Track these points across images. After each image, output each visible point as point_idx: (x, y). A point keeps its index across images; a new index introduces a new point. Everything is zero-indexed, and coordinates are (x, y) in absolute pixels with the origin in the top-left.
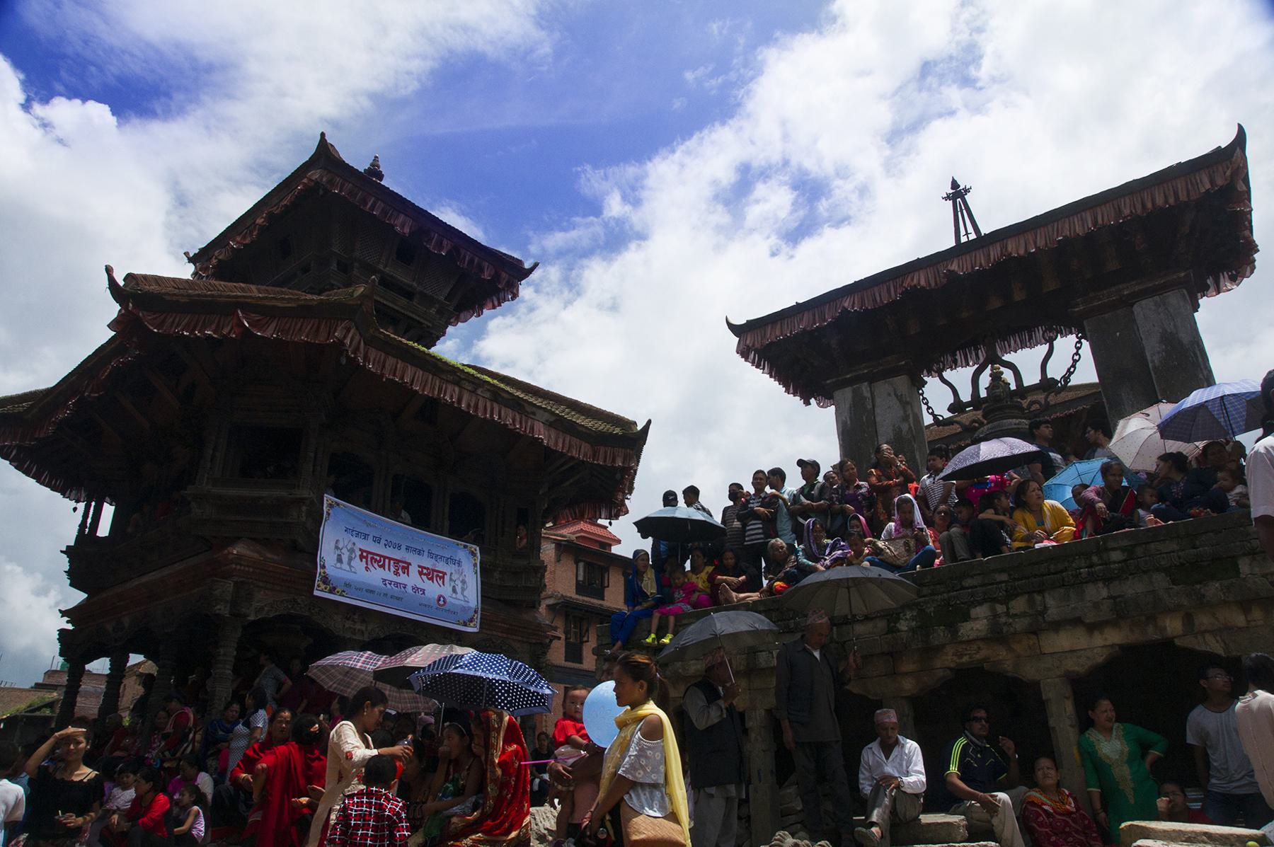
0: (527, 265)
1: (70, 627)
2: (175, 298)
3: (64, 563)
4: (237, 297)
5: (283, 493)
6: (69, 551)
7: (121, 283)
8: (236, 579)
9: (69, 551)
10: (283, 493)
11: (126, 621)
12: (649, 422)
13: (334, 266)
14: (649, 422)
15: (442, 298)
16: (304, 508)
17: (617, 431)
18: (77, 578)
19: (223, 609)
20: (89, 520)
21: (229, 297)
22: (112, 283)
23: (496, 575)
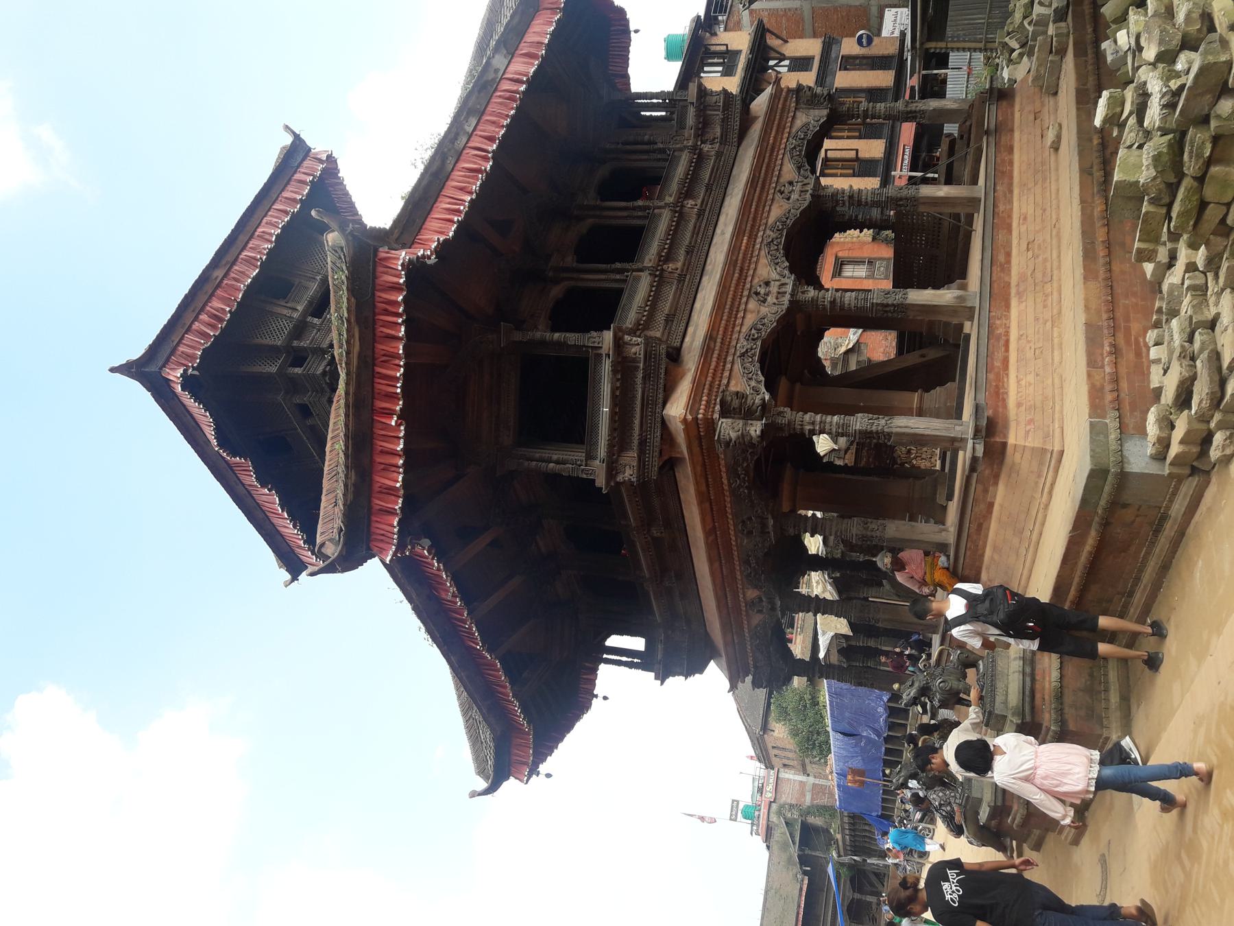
1: (749, 679)
2: (351, 489)
3: (675, 681)
4: (347, 406)
5: (606, 366)
6: (662, 677)
8: (716, 416)
9: (662, 677)
10: (606, 366)
11: (752, 594)
13: (298, 370)
16: (627, 338)
18: (694, 667)
19: (756, 429)
20: (624, 659)
21: (347, 415)
23: (706, 148)
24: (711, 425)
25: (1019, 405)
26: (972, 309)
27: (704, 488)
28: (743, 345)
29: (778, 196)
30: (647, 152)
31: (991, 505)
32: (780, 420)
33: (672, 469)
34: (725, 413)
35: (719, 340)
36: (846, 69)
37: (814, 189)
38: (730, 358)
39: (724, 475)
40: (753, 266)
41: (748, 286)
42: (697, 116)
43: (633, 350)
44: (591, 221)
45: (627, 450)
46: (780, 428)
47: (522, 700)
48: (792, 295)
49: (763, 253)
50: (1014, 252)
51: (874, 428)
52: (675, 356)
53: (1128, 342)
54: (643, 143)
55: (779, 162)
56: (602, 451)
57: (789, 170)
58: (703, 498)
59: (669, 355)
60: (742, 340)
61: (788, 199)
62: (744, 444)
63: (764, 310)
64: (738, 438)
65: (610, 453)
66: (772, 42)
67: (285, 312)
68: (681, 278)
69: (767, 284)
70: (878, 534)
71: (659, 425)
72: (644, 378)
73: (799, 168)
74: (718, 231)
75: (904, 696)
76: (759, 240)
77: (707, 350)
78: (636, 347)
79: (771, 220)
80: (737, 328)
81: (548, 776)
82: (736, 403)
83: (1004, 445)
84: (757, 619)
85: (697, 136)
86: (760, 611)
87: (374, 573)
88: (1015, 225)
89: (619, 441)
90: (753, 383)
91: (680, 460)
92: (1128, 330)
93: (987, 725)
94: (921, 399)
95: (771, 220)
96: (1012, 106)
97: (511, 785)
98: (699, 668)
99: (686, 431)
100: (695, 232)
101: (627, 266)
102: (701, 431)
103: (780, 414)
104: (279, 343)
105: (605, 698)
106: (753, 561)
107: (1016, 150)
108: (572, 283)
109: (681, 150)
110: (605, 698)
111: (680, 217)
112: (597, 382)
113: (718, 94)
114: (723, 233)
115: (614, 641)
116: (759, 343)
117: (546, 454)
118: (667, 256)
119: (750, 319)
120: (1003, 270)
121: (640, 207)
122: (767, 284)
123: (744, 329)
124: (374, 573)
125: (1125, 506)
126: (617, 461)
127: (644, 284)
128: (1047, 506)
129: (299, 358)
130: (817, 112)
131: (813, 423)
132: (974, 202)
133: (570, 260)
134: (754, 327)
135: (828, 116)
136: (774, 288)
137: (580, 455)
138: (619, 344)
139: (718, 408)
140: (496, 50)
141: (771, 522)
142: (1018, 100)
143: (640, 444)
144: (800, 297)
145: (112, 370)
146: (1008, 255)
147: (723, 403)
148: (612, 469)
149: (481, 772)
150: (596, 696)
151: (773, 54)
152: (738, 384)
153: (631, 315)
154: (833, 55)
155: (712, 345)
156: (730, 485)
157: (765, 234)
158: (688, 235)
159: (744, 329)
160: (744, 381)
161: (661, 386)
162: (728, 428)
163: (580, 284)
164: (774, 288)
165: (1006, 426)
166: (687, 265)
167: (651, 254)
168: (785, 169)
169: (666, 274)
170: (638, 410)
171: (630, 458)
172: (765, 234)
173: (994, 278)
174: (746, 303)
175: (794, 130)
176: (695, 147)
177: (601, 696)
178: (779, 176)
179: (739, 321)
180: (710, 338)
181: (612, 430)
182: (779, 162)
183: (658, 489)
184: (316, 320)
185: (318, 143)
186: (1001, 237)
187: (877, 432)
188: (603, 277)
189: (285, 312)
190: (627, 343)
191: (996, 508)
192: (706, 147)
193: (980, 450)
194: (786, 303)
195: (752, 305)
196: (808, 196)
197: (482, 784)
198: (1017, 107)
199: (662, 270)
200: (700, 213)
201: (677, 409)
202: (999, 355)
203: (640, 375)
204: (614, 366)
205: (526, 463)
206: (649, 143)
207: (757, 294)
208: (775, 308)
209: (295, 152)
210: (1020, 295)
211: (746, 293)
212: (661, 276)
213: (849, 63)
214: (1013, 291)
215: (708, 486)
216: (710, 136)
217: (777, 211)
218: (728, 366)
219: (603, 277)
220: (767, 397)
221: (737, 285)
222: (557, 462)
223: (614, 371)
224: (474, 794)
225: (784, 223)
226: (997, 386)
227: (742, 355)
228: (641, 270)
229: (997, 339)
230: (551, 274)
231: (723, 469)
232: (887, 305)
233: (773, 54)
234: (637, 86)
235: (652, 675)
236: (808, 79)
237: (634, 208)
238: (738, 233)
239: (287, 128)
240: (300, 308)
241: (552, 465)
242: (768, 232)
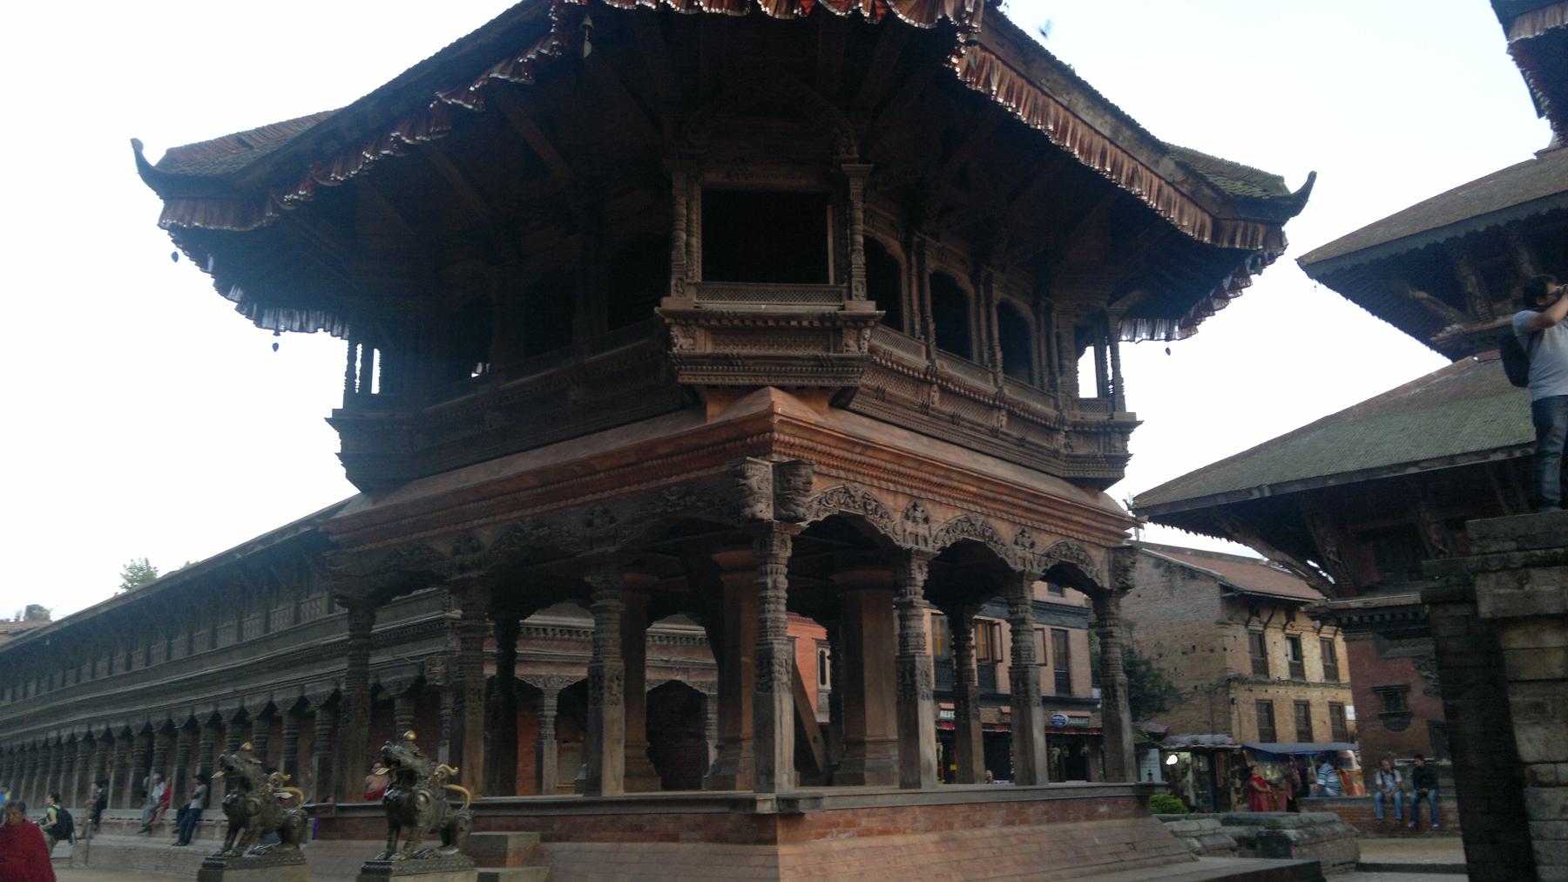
3: (332, 441)
5: (829, 308)
6: (337, 420)
8: (776, 458)
9: (337, 420)
11: (486, 537)
12: (1312, 177)
14: (1312, 177)
17: (1257, 192)
19: (764, 510)
20: (358, 365)
23: (1061, 439)
24: (763, 450)
25: (824, 855)
26: (918, 784)
27: (661, 451)
28: (859, 490)
29: (1018, 529)
30: (1050, 365)
31: (674, 838)
33: (683, 407)
34: (779, 468)
35: (863, 459)
37: (1030, 574)
38: (842, 474)
39: (683, 477)
40: (944, 500)
41: (923, 495)
42: (1099, 425)
43: (851, 343)
44: (971, 291)
45: (714, 341)
47: (275, 218)
48: (918, 551)
49: (958, 513)
51: (777, 667)
52: (840, 400)
54: (1060, 359)
55: (1053, 529)
57: (1046, 542)
58: (646, 451)
59: (845, 389)
60: (865, 489)
61: (1016, 543)
63: (898, 517)
64: (750, 489)
65: (710, 315)
68: (925, 409)
69: (926, 520)
70: (606, 695)
71: (753, 381)
72: (816, 358)
73: (1048, 555)
75: (397, 748)
76: (972, 507)
77: (850, 442)
78: (852, 347)
79: (993, 522)
80: (876, 483)
82: (799, 482)
83: (773, 841)
84: (444, 548)
85: (1075, 425)
86: (456, 551)
88: (1016, 829)
90: (815, 506)
93: (364, 871)
95: (993, 522)
97: (154, 204)
98: (351, 477)
100: (975, 426)
101: (932, 338)
102: (754, 437)
103: (784, 541)
105: (276, 347)
106: (544, 532)
108: (904, 266)
109: (1056, 407)
110: (276, 347)
111: (991, 406)
112: (805, 297)
113: (1125, 448)
114: (976, 461)
116: (861, 512)
117: (697, 228)
119: (888, 501)
120: (967, 818)
121: (994, 355)
122: (926, 520)
123: (875, 492)
126: (700, 326)
127: (919, 361)
130: (1106, 574)
131: (775, 587)
132: (1029, 777)
133: (931, 265)
135: (1102, 589)
136: (922, 530)
137: (697, 274)
138: (859, 322)
139: (786, 459)
141: (612, 549)
142: (1141, 821)
143: (726, 357)
148: (690, 319)
149: (173, 156)
150: (277, 334)
152: (819, 487)
155: (858, 450)
156: (668, 487)
161: (806, 382)
162: (760, 474)
163: (904, 279)
164: (922, 530)
166: (937, 417)
167: (945, 366)
168: (1045, 537)
169: (926, 389)
170: (771, 352)
171: (705, 346)
173: (956, 809)
174: (904, 493)
175: (1086, 546)
177: (281, 339)
178: (1038, 529)
179: (884, 485)
180: (868, 446)
181: (742, 317)
182: (1053, 529)
183: (660, 388)
186: (1000, 814)
187: (771, 672)
188: (915, 307)
190: (860, 330)
191: (673, 846)
193: (765, 808)
194: (908, 546)
195: (903, 502)
196: (1019, 568)
197: (154, 157)
199: (931, 384)
200: (995, 432)
201: (783, 404)
202: (875, 823)
204: (832, 318)
205: (683, 201)
206: (1061, 366)
207: (915, 507)
208: (898, 529)
210: (944, 840)
211: (915, 492)
212: (924, 382)
215: (667, 456)
216: (1075, 442)
217: (1005, 530)
218: (834, 472)
219: (915, 307)
220: (803, 524)
221: (924, 481)
222: (688, 245)
223: (823, 317)
224: (137, 145)
225: (991, 538)
226: (837, 825)
227: (847, 491)
228: (928, 356)
230: (916, 239)
231: (692, 475)
232: (913, 675)
234: (1125, 347)
235: (340, 406)
237: (991, 348)
238: (981, 479)
241: (684, 236)
242: (982, 518)
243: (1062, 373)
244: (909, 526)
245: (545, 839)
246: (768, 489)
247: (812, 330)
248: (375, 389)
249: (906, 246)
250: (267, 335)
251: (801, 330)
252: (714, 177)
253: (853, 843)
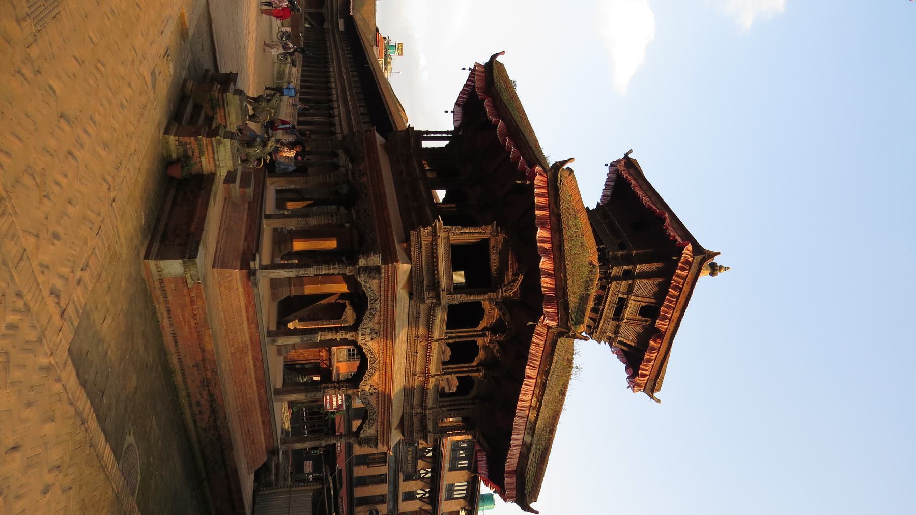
0: (656, 395)
7: (565, 167)
8: (383, 266)
13: (625, 267)
15: (619, 339)
17: (528, 488)
19: (362, 262)
22: (563, 163)
23: (419, 410)
24: (385, 261)
28: (377, 305)
31: (246, 240)
32: (351, 268)
34: (378, 269)
36: (383, 495)
42: (426, 426)
44: (474, 364)
46: (350, 265)
50: (252, 367)
53: (189, 321)
56: (441, 243)
62: (367, 253)
63: (370, 325)
66: (428, 507)
67: (639, 299)
74: (403, 365)
81: (464, 69)
83: (241, 269)
87: (551, 162)
88: (254, 383)
89: (433, 246)
90: (368, 286)
91: (400, 242)
92: (190, 328)
94: (290, 291)
96: (267, 447)
97: (484, 60)
99: (396, 256)
100: (415, 363)
102: (390, 257)
104: (638, 281)
105: (446, 112)
107: (260, 424)
109: (432, 408)
110: (446, 112)
115: (443, 144)
118: (428, 348)
119: (376, 319)
123: (378, 314)
124: (551, 162)
125: (180, 244)
128: (218, 242)
129: (627, 275)
133: (480, 342)
134: (374, 316)
139: (383, 271)
140: (531, 444)
144: (353, 333)
145: (719, 253)
146: (255, 366)
147: (380, 273)
148: (434, 232)
149: (501, 66)
151: (426, 500)
152: (374, 283)
153: (440, 316)
154: (391, 503)
157: (379, 365)
158: (418, 361)
159: (378, 314)
160: (370, 285)
165: (242, 278)
166: (415, 345)
172: (379, 365)
176: (425, 410)
184: (622, 296)
185: (642, 396)
189: (639, 299)
191: (243, 238)
192: (419, 410)
193: (252, 264)
197: (499, 59)
198: (264, 446)
201: (404, 268)
203: (425, 283)
204: (439, 286)
209: (652, 387)
213: (381, 499)
214: (249, 347)
222: (465, 233)
223: (439, 282)
224: (503, 53)
229: (253, 320)
233: (426, 500)
236: (405, 487)
239: (659, 401)
240: (631, 302)
243: (448, 410)
244: (368, 331)
245: (250, 202)
246: (371, 263)
247: (434, 279)
248: (426, 144)
249: (485, 329)
250: (451, 107)
251: (434, 275)
252: (492, 242)
253: (243, 304)
